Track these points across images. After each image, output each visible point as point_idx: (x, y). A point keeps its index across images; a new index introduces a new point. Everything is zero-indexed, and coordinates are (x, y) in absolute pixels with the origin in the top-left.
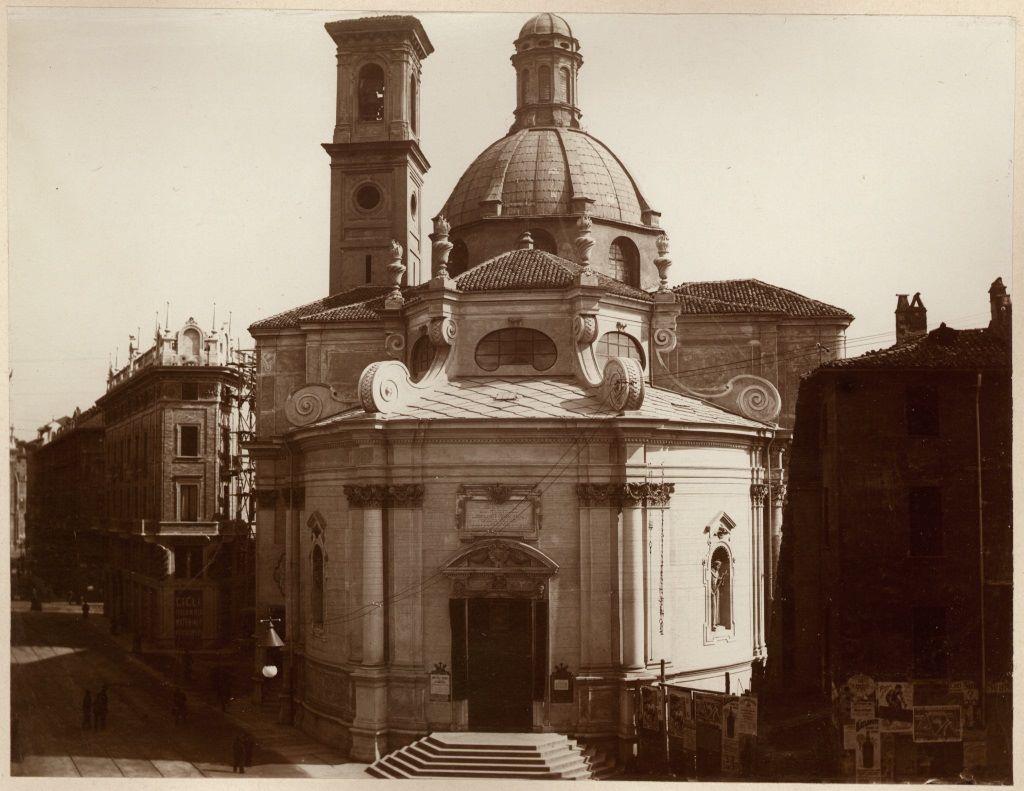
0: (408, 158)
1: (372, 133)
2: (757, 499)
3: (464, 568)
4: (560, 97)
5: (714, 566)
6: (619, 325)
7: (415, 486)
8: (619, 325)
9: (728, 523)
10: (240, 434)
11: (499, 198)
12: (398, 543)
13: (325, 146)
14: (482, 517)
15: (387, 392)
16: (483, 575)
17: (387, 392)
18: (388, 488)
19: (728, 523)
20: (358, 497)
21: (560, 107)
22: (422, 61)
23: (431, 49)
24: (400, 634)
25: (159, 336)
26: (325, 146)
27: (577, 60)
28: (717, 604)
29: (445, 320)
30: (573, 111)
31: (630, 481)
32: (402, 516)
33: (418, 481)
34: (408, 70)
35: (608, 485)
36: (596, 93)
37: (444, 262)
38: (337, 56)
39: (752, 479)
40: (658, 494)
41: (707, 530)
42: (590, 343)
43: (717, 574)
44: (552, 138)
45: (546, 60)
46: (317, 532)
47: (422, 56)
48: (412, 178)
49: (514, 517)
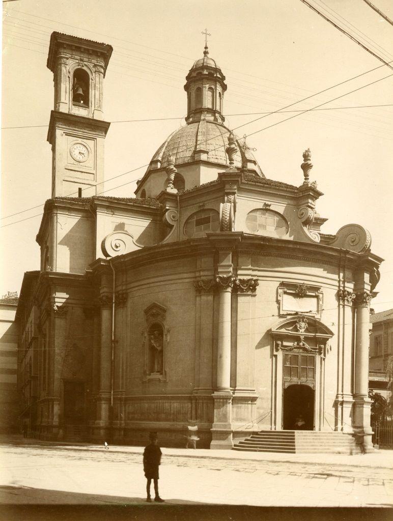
27: (224, 87)
37: (171, 180)
49: (306, 306)
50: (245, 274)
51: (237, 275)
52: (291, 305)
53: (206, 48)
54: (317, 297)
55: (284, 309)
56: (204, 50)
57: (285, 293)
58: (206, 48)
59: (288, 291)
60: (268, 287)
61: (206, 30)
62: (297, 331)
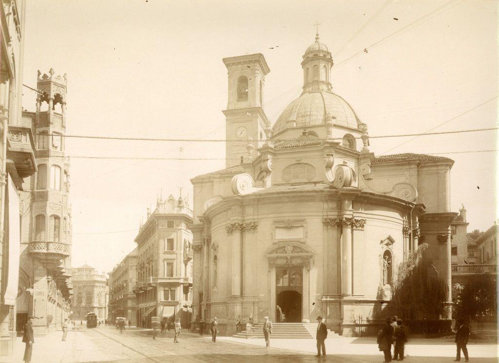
0: (258, 115)
1: (243, 105)
2: (406, 233)
3: (274, 255)
4: (323, 78)
5: (384, 258)
6: (344, 162)
7: (254, 223)
8: (344, 162)
9: (391, 241)
10: (192, 246)
11: (295, 119)
12: (247, 247)
13: (223, 111)
14: (282, 235)
15: (243, 186)
16: (281, 258)
18: (243, 224)
19: (391, 241)
20: (231, 230)
21: (323, 82)
22: (265, 76)
23: (269, 71)
24: (248, 281)
25: (158, 203)
26: (223, 111)
28: (386, 274)
29: (269, 161)
30: (328, 84)
31: (345, 216)
32: (248, 236)
33: (256, 220)
34: (258, 78)
35: (336, 219)
36: (339, 76)
39: (404, 225)
40: (355, 224)
41: (382, 242)
42: (331, 167)
43: (386, 262)
44: (318, 95)
45: (316, 63)
46: (215, 250)
47: (265, 74)
48: (260, 124)
49: (296, 234)
51: (245, 220)
52: (282, 235)
53: (317, 35)
54: (302, 226)
55: (276, 238)
56: (316, 36)
57: (277, 227)
58: (317, 35)
59: (279, 226)
60: (265, 226)
61: (317, 22)
62: (286, 253)
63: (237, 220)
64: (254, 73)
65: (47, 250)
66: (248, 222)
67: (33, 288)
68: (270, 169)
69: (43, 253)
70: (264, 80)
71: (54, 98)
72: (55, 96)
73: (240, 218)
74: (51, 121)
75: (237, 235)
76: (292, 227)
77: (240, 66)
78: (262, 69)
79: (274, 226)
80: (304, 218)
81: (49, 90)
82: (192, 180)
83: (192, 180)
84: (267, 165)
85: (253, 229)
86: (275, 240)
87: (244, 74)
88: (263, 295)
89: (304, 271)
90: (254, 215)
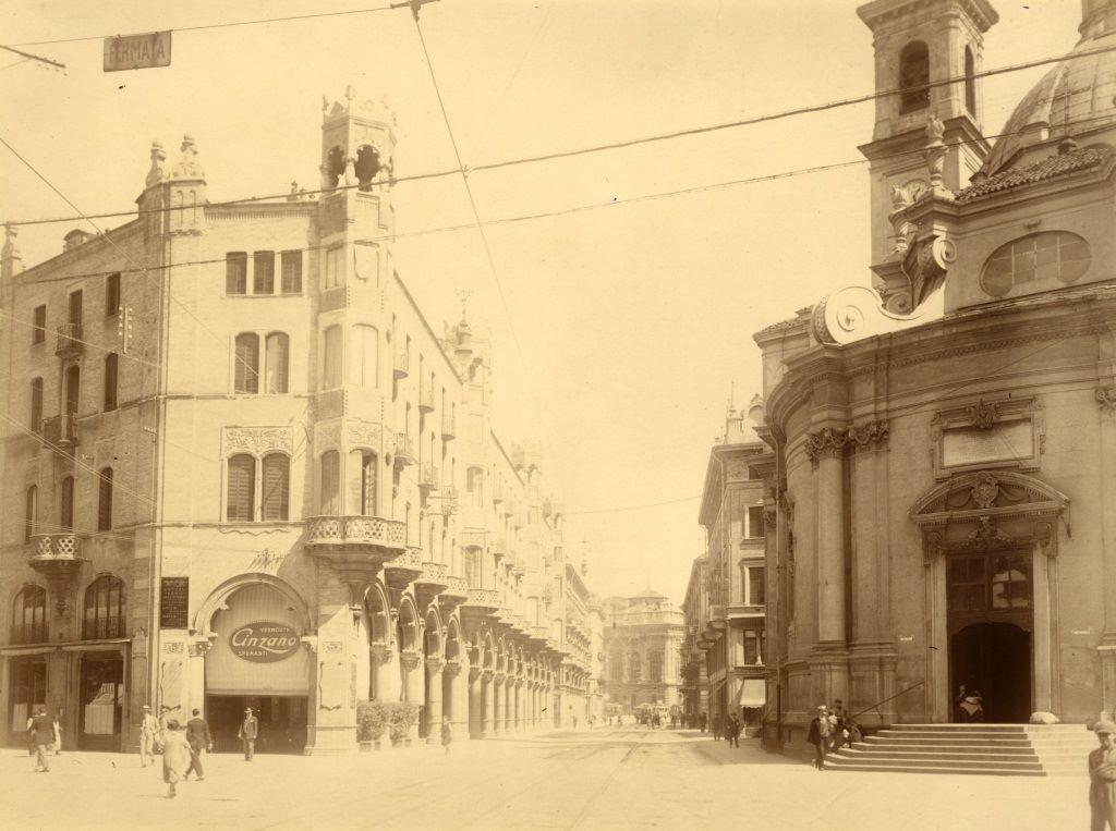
3: (940, 516)
7: (879, 424)
12: (861, 498)
15: (848, 320)
17: (848, 320)
18: (848, 431)
22: (984, 35)
33: (883, 417)
38: (874, 45)
47: (983, 28)
50: (864, 412)
51: (852, 420)
52: (960, 453)
54: (1027, 420)
55: (947, 464)
57: (946, 431)
59: (952, 426)
60: (912, 431)
63: (830, 419)
64: (944, 28)
65: (343, 537)
66: (859, 423)
67: (316, 633)
68: (943, 266)
69: (335, 546)
70: (979, 45)
71: (356, 157)
72: (359, 152)
73: (838, 415)
74: (350, 215)
75: (831, 465)
76: (993, 424)
77: (905, 18)
78: (970, 14)
79: (936, 428)
80: (1031, 392)
81: (346, 141)
82: (757, 337)
83: (757, 337)
84: (931, 253)
85: (878, 442)
86: (942, 468)
87: (917, 38)
88: (911, 639)
89: (1039, 563)
90: (876, 402)
